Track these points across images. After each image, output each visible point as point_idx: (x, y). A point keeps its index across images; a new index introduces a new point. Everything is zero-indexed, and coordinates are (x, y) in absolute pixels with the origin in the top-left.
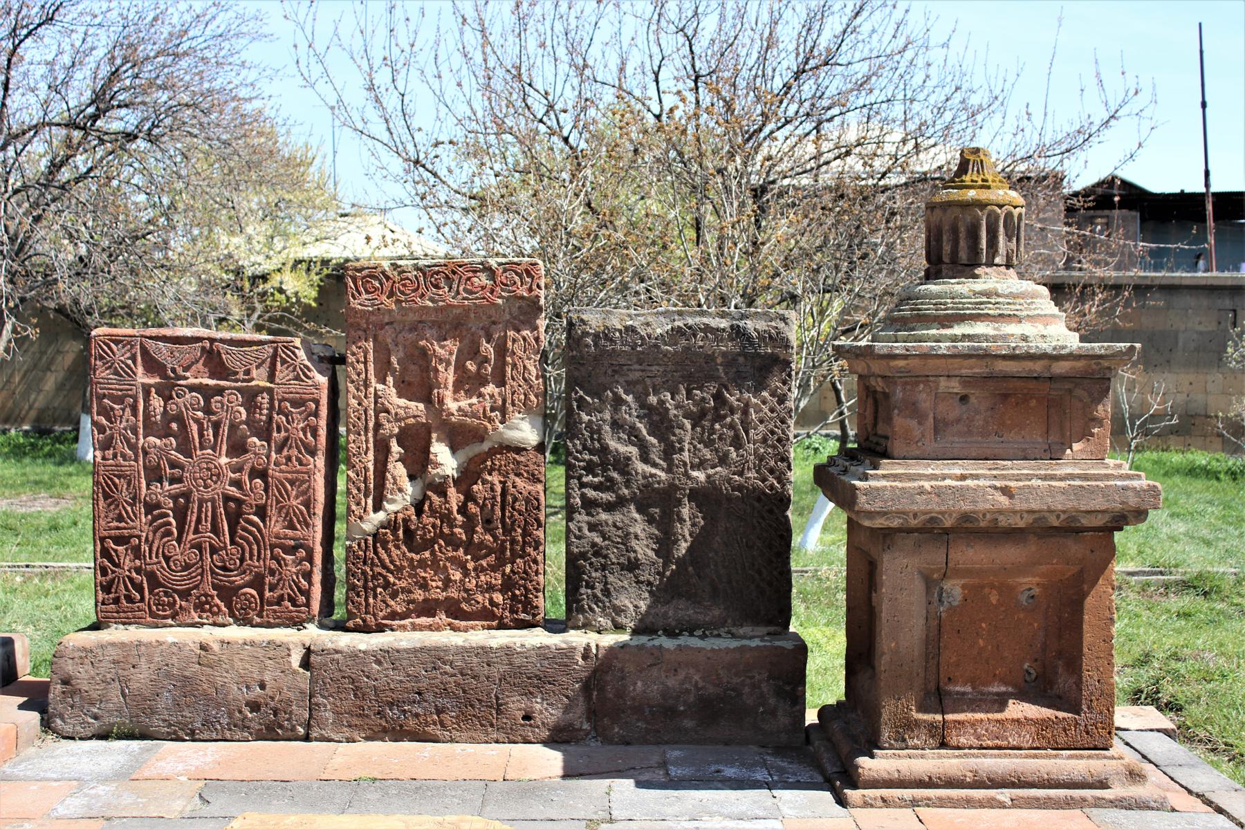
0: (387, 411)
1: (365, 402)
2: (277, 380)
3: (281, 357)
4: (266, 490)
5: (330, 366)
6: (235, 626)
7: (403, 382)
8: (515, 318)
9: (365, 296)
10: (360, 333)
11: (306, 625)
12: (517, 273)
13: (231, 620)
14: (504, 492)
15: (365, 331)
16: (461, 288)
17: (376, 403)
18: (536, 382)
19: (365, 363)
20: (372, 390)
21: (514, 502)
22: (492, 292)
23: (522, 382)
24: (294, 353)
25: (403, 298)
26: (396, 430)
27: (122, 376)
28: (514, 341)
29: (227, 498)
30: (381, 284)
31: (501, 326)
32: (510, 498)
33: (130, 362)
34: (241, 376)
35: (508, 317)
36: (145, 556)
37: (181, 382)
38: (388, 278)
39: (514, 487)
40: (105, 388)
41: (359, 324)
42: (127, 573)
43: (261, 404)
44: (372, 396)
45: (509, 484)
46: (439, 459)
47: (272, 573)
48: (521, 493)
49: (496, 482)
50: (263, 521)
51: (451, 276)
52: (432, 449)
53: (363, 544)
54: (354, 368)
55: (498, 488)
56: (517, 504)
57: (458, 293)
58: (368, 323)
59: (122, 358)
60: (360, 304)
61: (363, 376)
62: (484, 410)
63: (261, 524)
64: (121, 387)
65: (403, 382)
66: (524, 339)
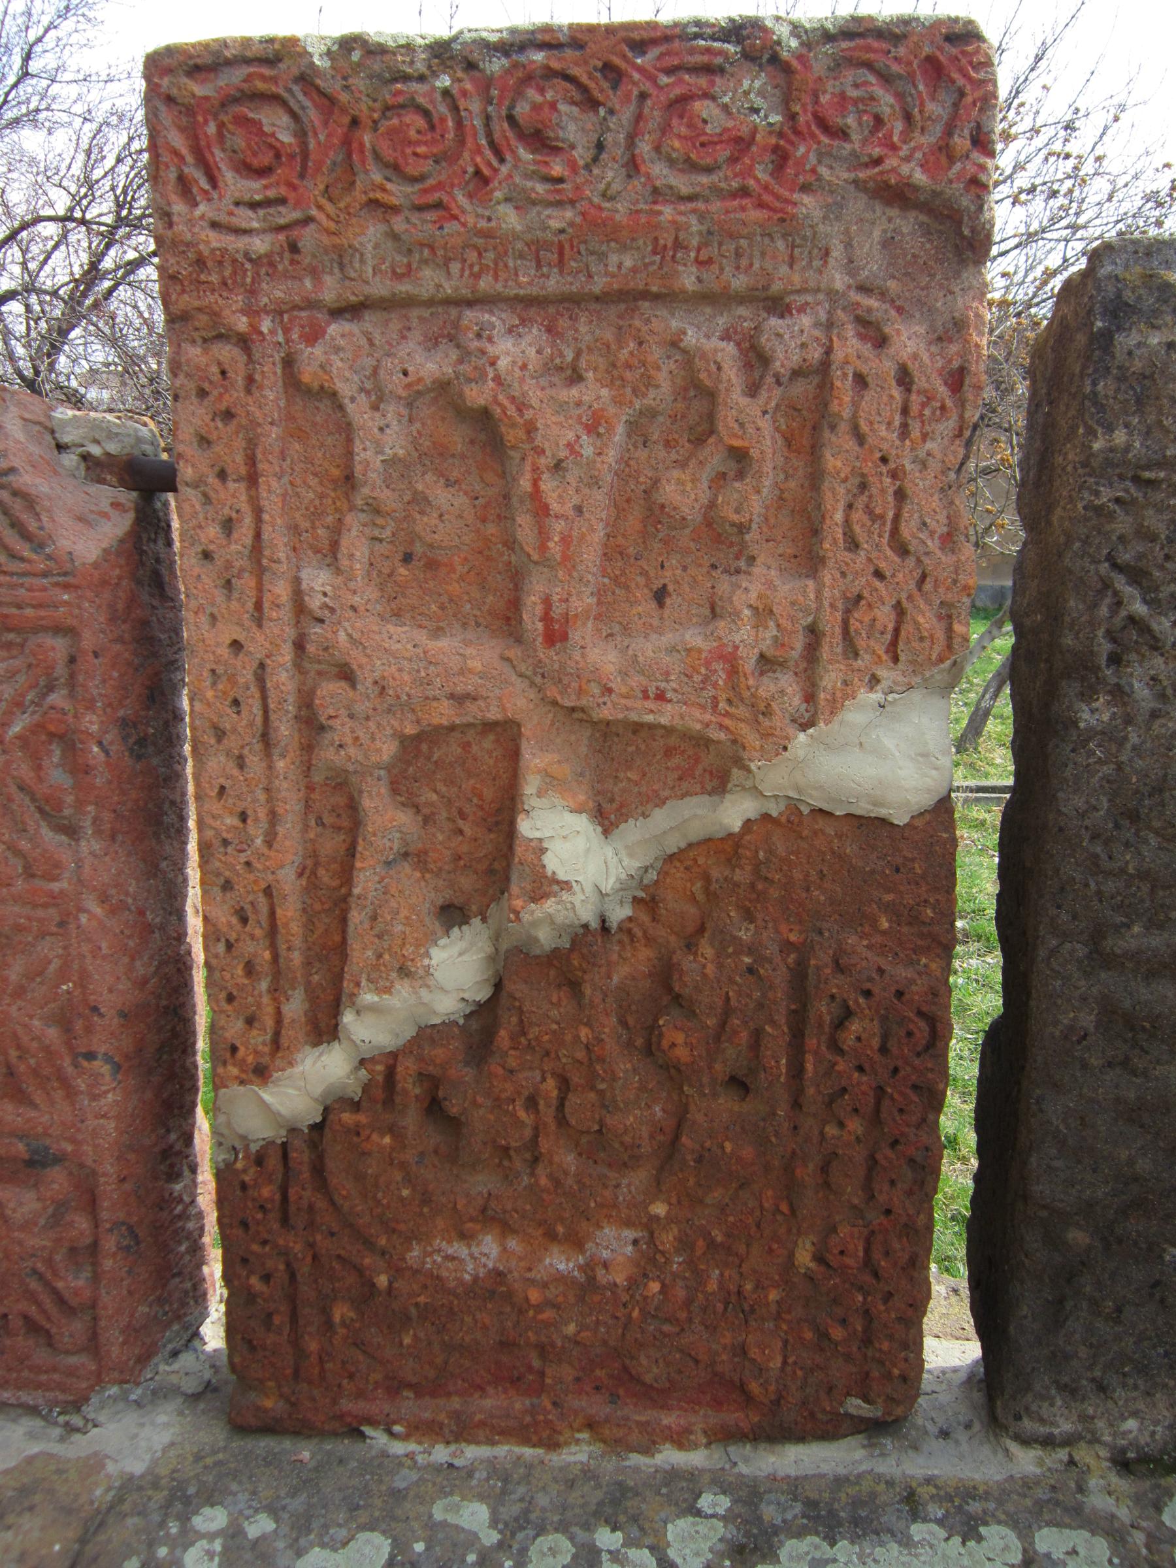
0: (346, 674)
1: (257, 645)
5: (128, 497)
7: (407, 558)
8: (863, 289)
9: (235, 184)
10: (227, 352)
12: (886, 79)
14: (799, 976)
15: (244, 342)
16: (644, 147)
17: (299, 646)
18: (947, 559)
19: (252, 479)
20: (281, 590)
21: (840, 1024)
22: (781, 158)
23: (888, 560)
25: (398, 193)
26: (388, 749)
28: (861, 381)
30: (301, 134)
31: (806, 321)
32: (823, 1010)
35: (839, 280)
38: (328, 102)
39: (839, 968)
41: (215, 315)
44: (286, 613)
45: (821, 959)
46: (552, 863)
48: (868, 994)
49: (772, 949)
51: (599, 87)
52: (526, 827)
53: (274, 1162)
54: (207, 499)
55: (779, 975)
56: (855, 1027)
57: (633, 166)
58: (251, 312)
60: (214, 225)
61: (244, 532)
62: (733, 671)
65: (407, 558)
66: (904, 378)
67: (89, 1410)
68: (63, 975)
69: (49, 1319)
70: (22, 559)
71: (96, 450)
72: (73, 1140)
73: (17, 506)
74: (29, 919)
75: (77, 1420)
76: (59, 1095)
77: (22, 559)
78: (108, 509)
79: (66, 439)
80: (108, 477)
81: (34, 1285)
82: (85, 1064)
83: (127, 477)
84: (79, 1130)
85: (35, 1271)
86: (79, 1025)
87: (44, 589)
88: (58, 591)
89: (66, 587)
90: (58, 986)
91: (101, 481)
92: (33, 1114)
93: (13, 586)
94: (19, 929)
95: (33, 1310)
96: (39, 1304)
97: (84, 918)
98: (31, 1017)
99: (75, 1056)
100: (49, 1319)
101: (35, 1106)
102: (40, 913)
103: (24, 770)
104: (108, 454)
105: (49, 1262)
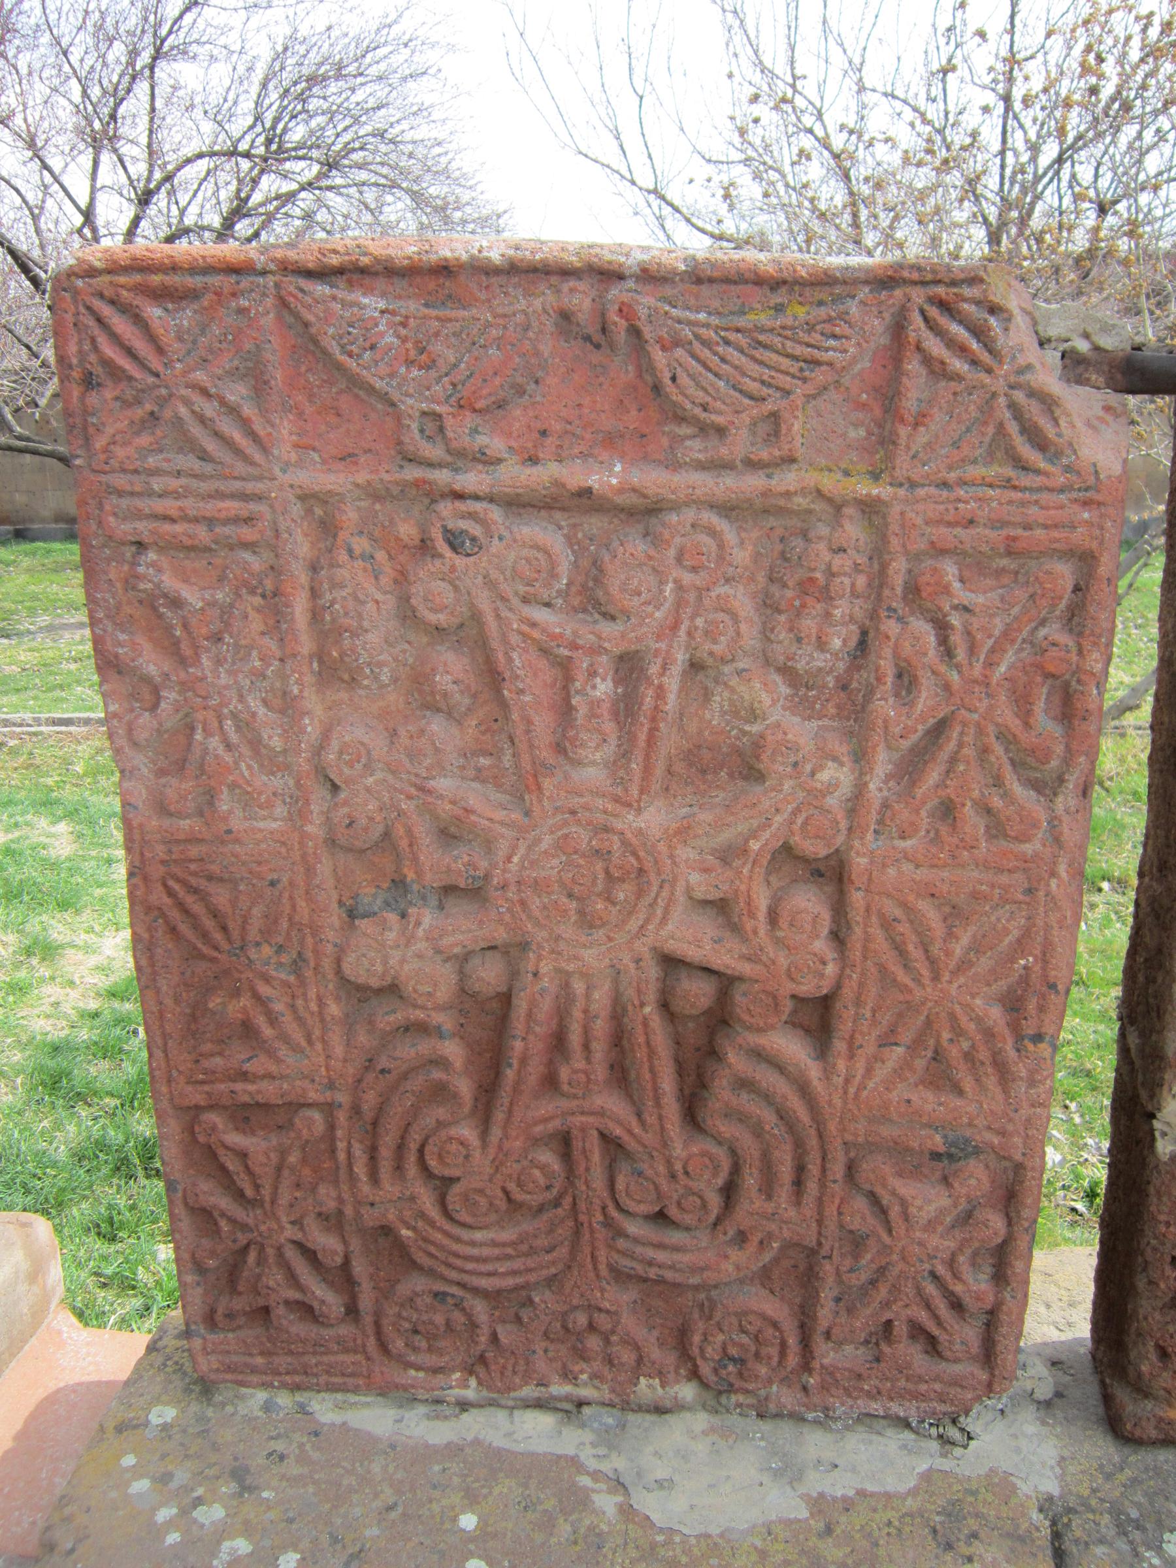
2: (903, 466)
3: (927, 360)
4: (838, 937)
6: (701, 1420)
11: (967, 1422)
13: (687, 1391)
24: (979, 332)
27: (204, 456)
29: (671, 963)
33: (237, 392)
34: (740, 444)
36: (352, 1178)
37: (471, 480)
40: (139, 515)
42: (290, 1232)
43: (831, 574)
47: (856, 1243)
50: (823, 1049)
59: (199, 376)
63: (814, 1071)
64: (210, 508)
67: (967, 1422)
68: (1020, 947)
69: (940, 1324)
70: (1038, 472)
71: (1083, 346)
72: (1002, 1133)
73: (1033, 409)
74: (993, 886)
75: (953, 1433)
76: (991, 1082)
77: (1038, 472)
78: (1101, 413)
79: (1052, 332)
80: (1094, 377)
81: (931, 1289)
82: (1031, 1047)
83: (1119, 376)
84: (1010, 1120)
85: (933, 1275)
86: (1032, 1005)
87: (1062, 507)
88: (1076, 508)
89: (1086, 503)
90: (1013, 960)
91: (1080, 381)
92: (959, 1102)
93: (1023, 504)
94: (975, 896)
95: (923, 1316)
96: (928, 1306)
97: (1054, 883)
98: (973, 996)
99: (1019, 1037)
100: (940, 1324)
101: (961, 1093)
102: (1004, 879)
103: (1007, 715)
104: (1097, 348)
105: (951, 1263)
